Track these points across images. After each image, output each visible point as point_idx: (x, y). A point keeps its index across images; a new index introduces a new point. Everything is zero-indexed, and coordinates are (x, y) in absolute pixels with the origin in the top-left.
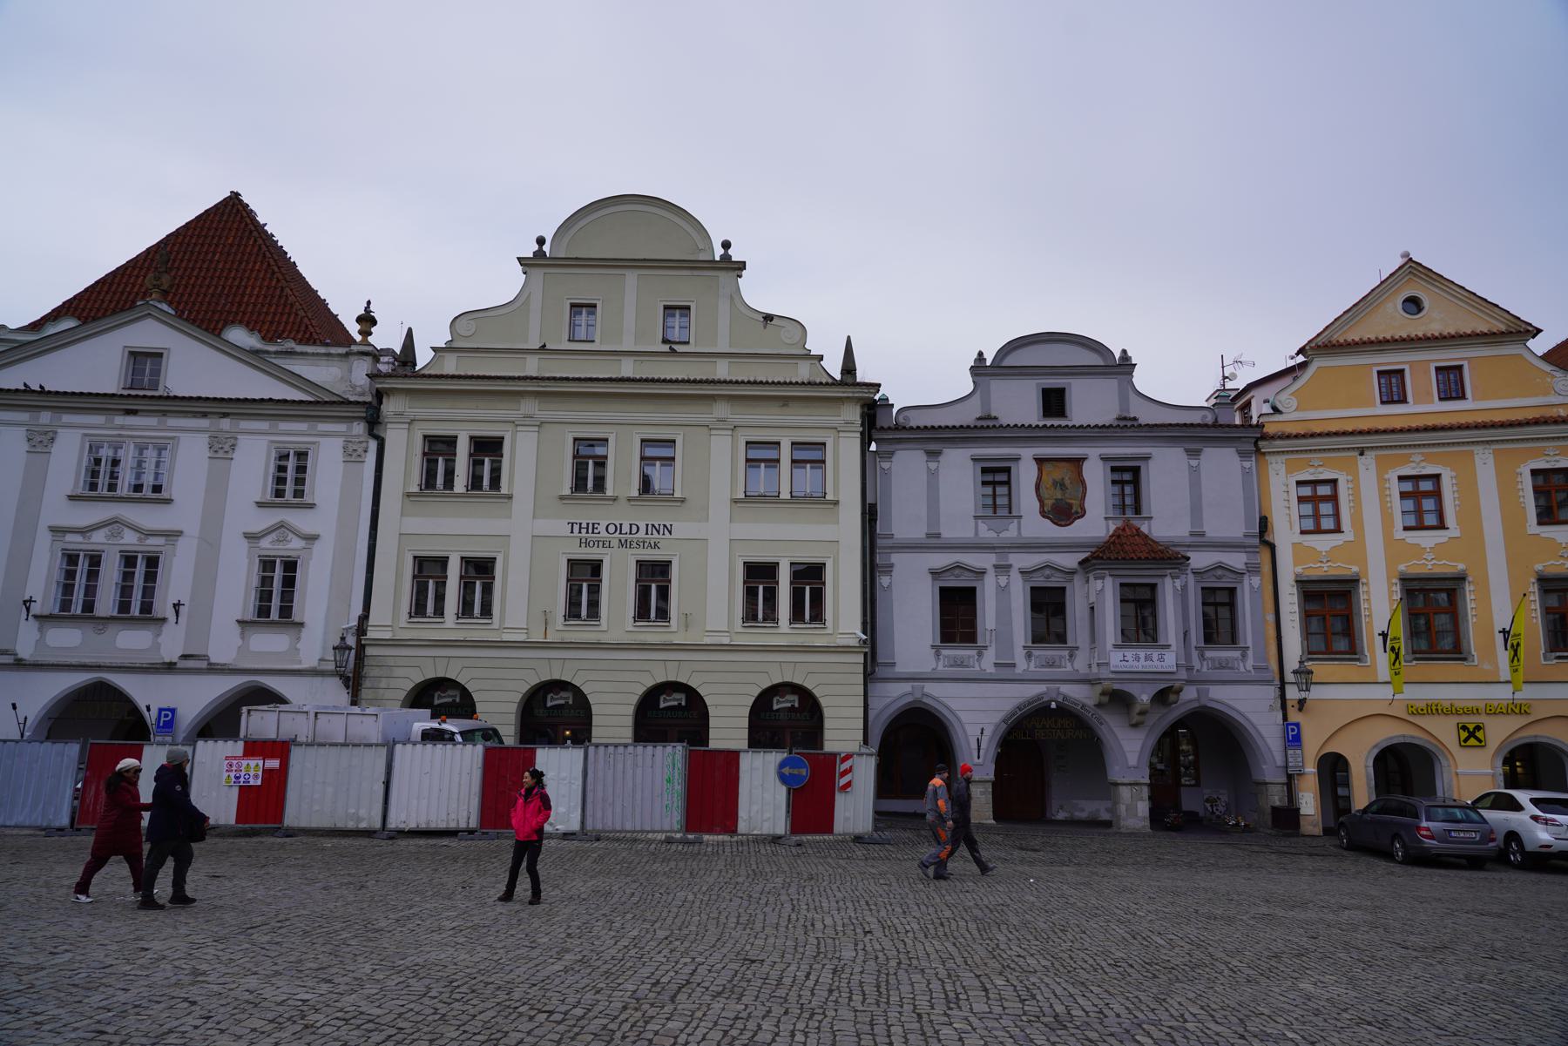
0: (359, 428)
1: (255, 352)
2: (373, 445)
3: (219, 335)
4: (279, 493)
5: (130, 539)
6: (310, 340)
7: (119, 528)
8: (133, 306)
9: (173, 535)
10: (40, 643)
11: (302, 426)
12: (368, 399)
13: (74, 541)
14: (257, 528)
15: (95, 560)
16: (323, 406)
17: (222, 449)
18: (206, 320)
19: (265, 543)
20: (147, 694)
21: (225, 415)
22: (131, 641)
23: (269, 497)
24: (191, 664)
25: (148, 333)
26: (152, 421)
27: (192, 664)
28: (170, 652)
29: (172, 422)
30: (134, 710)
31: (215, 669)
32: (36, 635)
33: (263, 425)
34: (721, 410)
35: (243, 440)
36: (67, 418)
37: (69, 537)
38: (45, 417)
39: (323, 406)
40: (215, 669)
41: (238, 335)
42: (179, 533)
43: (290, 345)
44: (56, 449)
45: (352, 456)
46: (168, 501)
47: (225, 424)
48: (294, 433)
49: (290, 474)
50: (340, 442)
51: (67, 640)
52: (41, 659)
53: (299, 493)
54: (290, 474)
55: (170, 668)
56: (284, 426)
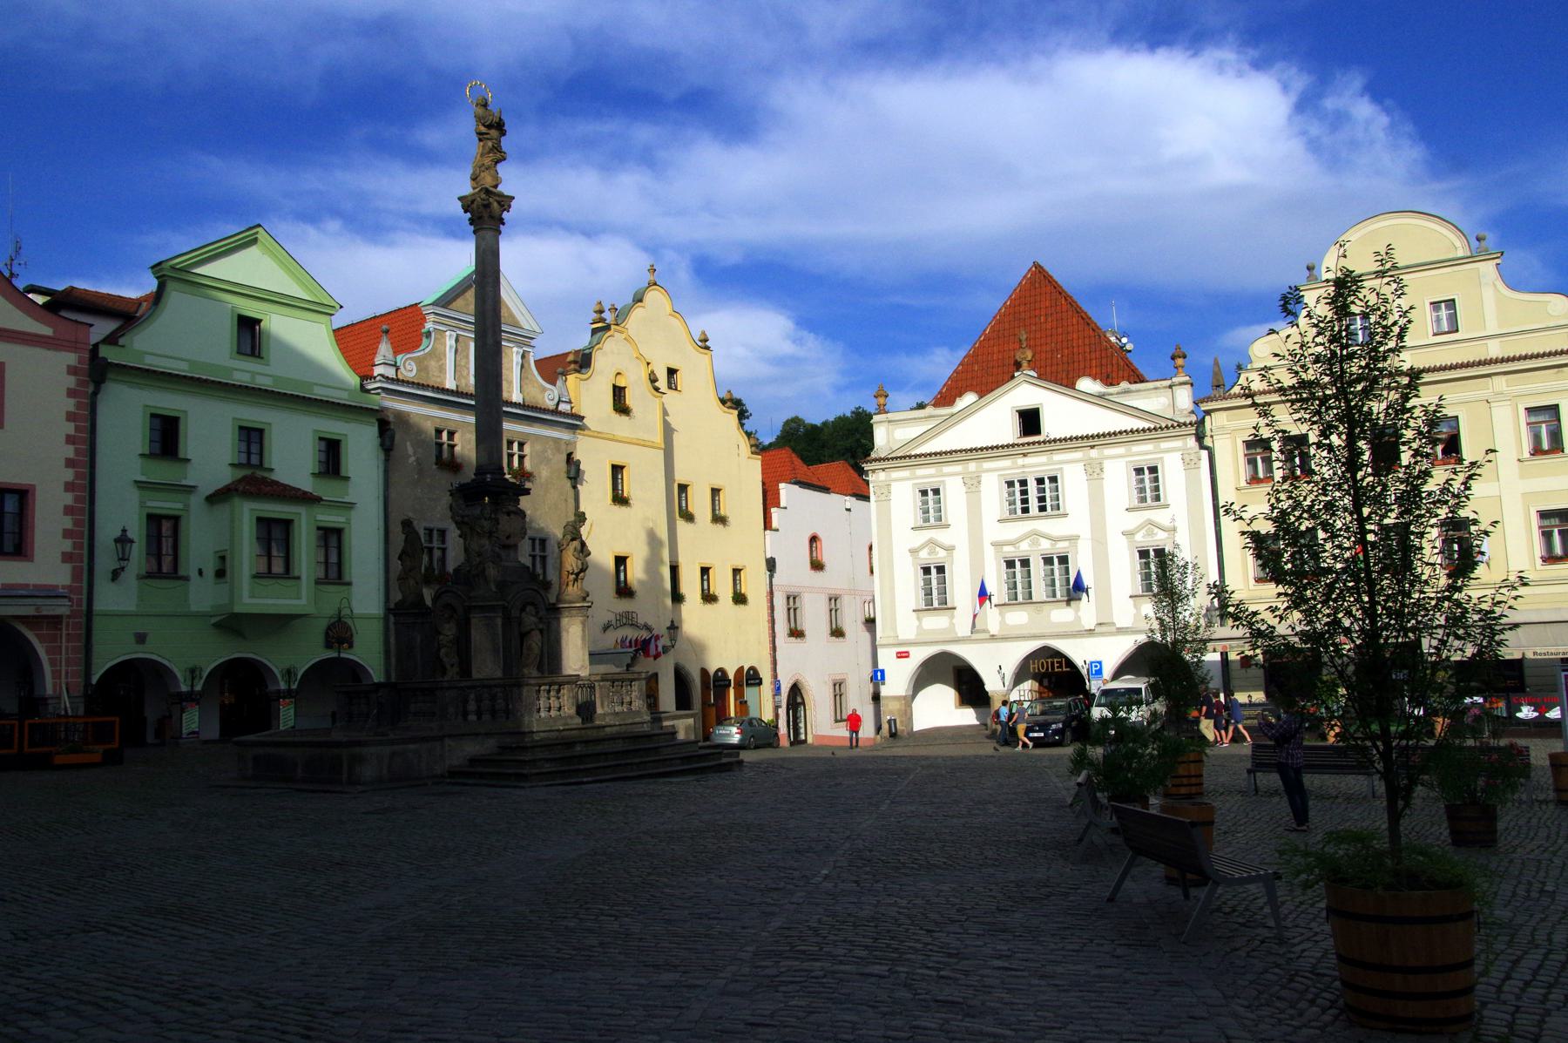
0: (1191, 442)
1: (1101, 396)
2: (1204, 454)
3: (1072, 386)
4: (1143, 500)
5: (1046, 546)
6: (1138, 378)
7: (1035, 536)
8: (1013, 377)
9: (1073, 539)
10: (1003, 622)
11: (1149, 447)
12: (1194, 418)
13: (1010, 552)
14: (1130, 527)
15: (1025, 563)
16: (1161, 428)
17: (1094, 472)
18: (1061, 376)
19: (1139, 537)
20: (1079, 653)
21: (1092, 447)
22: (1062, 615)
23: (1136, 503)
24: (1103, 629)
25: (1024, 392)
26: (1043, 459)
27: (1103, 628)
28: (1089, 622)
29: (1057, 457)
30: (1070, 663)
31: (1121, 631)
32: (999, 618)
33: (1120, 450)
34: (1500, 383)
35: (1107, 464)
36: (987, 465)
37: (1006, 549)
38: (972, 466)
39: (1161, 428)
40: (1121, 631)
41: (1086, 384)
42: (1078, 537)
43: (1124, 385)
44: (983, 486)
45: (1189, 464)
46: (1065, 515)
47: (1094, 453)
48: (1144, 452)
49: (1148, 484)
50: (1178, 455)
51: (1019, 617)
52: (1004, 633)
53: (1157, 498)
54: (1148, 484)
55: (1090, 632)
56: (1136, 448)
